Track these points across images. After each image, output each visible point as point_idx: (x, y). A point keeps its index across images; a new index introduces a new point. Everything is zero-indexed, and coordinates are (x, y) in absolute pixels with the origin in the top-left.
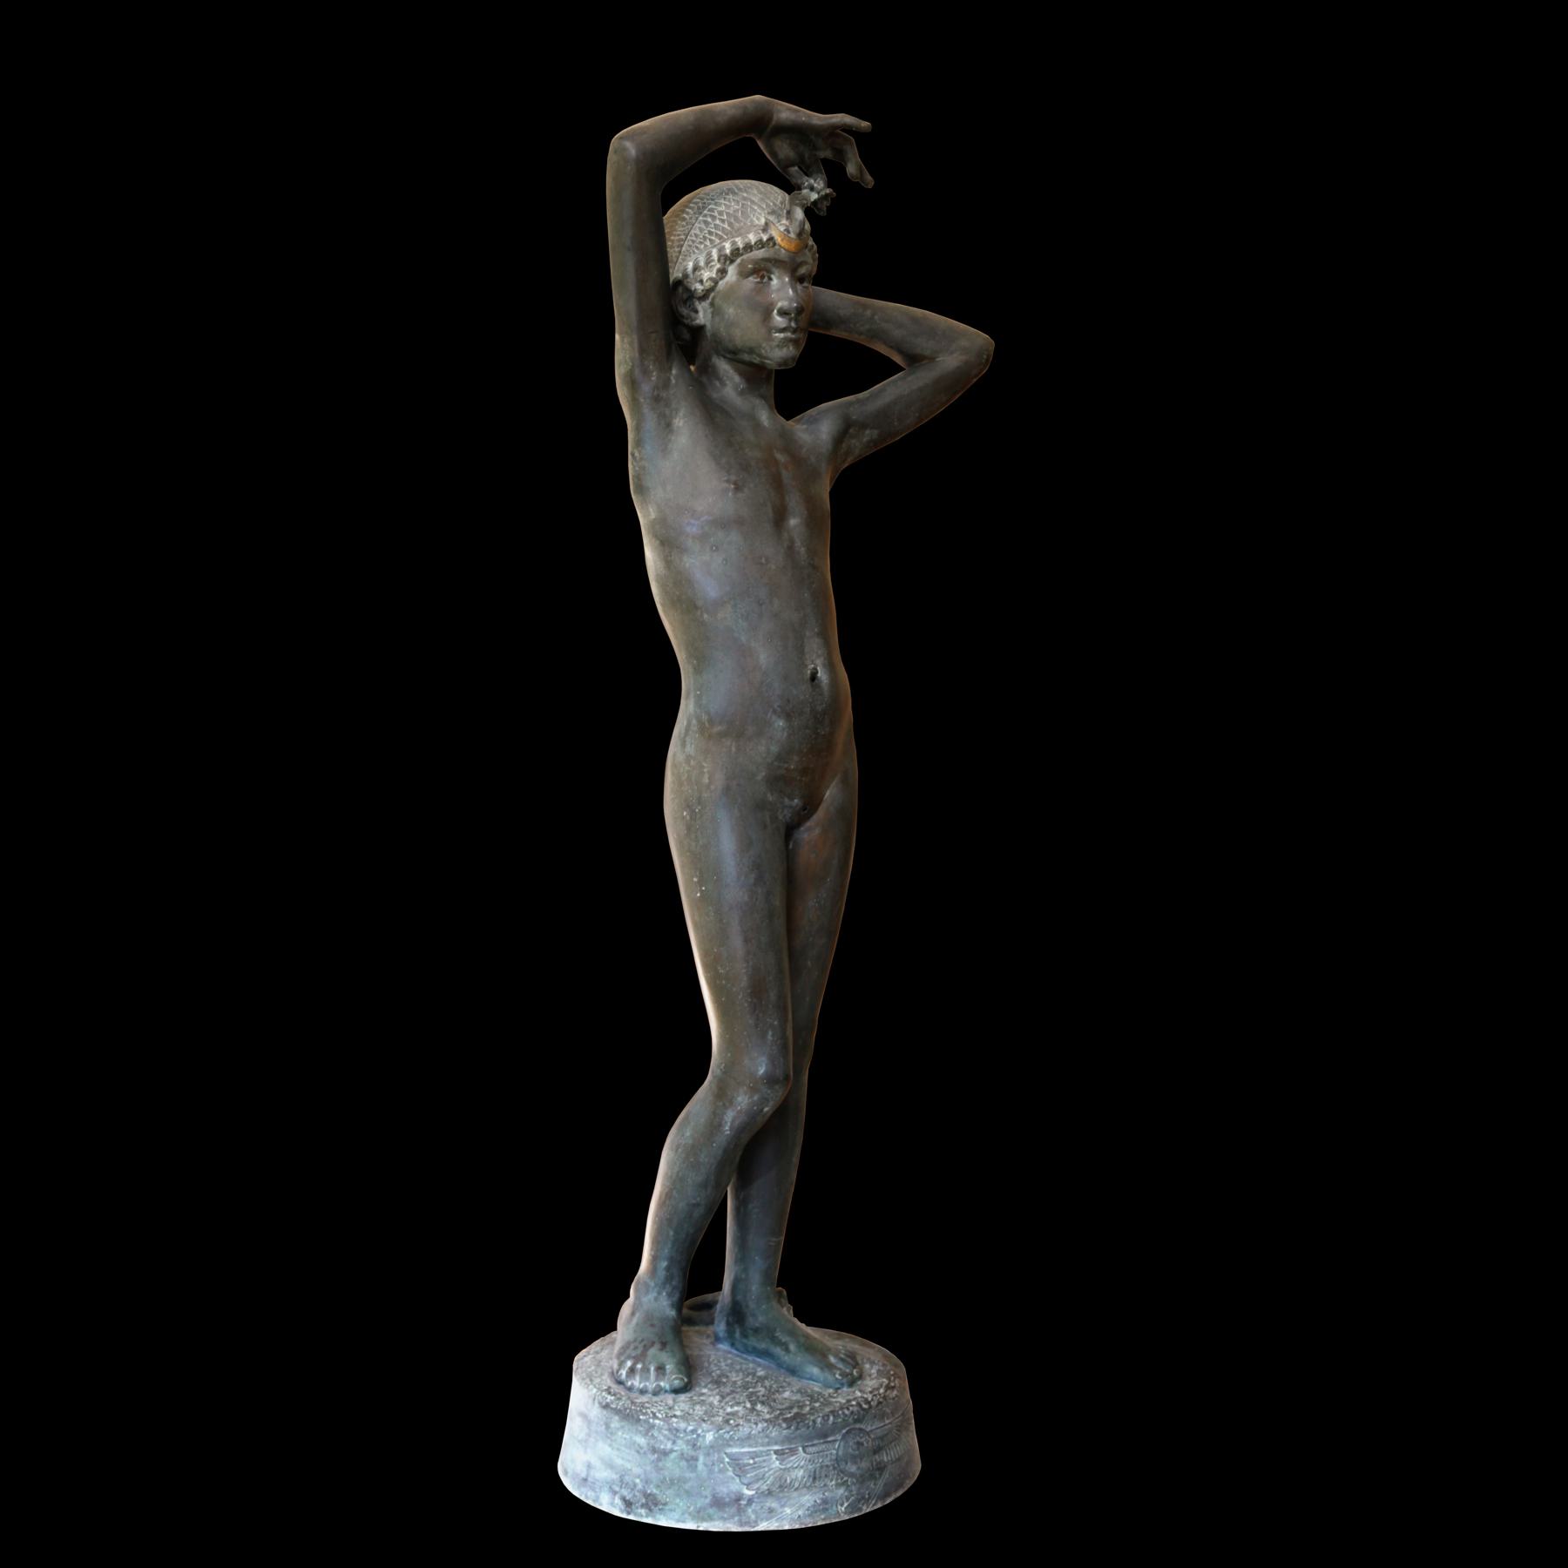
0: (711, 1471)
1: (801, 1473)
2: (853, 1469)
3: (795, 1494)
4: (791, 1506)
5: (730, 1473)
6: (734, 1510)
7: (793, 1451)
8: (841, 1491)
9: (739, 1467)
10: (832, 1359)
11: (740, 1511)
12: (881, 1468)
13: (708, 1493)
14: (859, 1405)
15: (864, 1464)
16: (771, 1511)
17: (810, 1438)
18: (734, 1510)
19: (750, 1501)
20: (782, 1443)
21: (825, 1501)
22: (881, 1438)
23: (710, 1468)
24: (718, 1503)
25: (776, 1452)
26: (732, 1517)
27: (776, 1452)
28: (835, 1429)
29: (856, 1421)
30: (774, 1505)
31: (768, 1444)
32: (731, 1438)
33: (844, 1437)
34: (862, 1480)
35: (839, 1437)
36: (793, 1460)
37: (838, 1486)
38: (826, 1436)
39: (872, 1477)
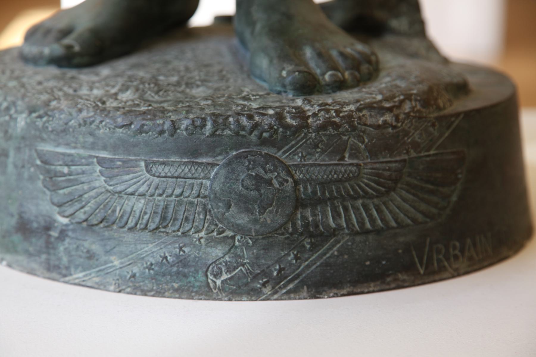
0: (20, 176)
1: (140, 204)
2: (243, 219)
3: (129, 237)
4: (122, 255)
5: (40, 184)
6: (41, 242)
7: (128, 166)
8: (217, 252)
9: (52, 180)
10: (308, 52)
11: (49, 247)
12: (319, 236)
13: (14, 209)
14: (279, 117)
15: (271, 218)
16: (91, 256)
17: (163, 151)
18: (41, 242)
19: (63, 234)
20: (115, 149)
21: (183, 262)
22: (323, 184)
23: (20, 167)
24: (24, 228)
25: (101, 161)
26: (39, 253)
27: (101, 161)
28: (214, 145)
29: (263, 142)
30: (96, 248)
31: (93, 146)
32: (45, 128)
33: (229, 163)
34: (267, 239)
35: (221, 160)
36: (126, 181)
37: (210, 241)
38: (195, 153)
39: (292, 243)
